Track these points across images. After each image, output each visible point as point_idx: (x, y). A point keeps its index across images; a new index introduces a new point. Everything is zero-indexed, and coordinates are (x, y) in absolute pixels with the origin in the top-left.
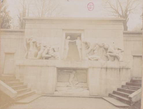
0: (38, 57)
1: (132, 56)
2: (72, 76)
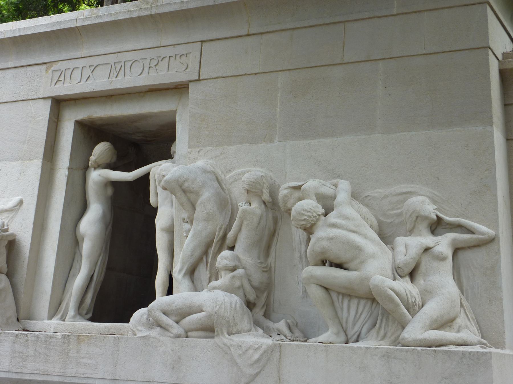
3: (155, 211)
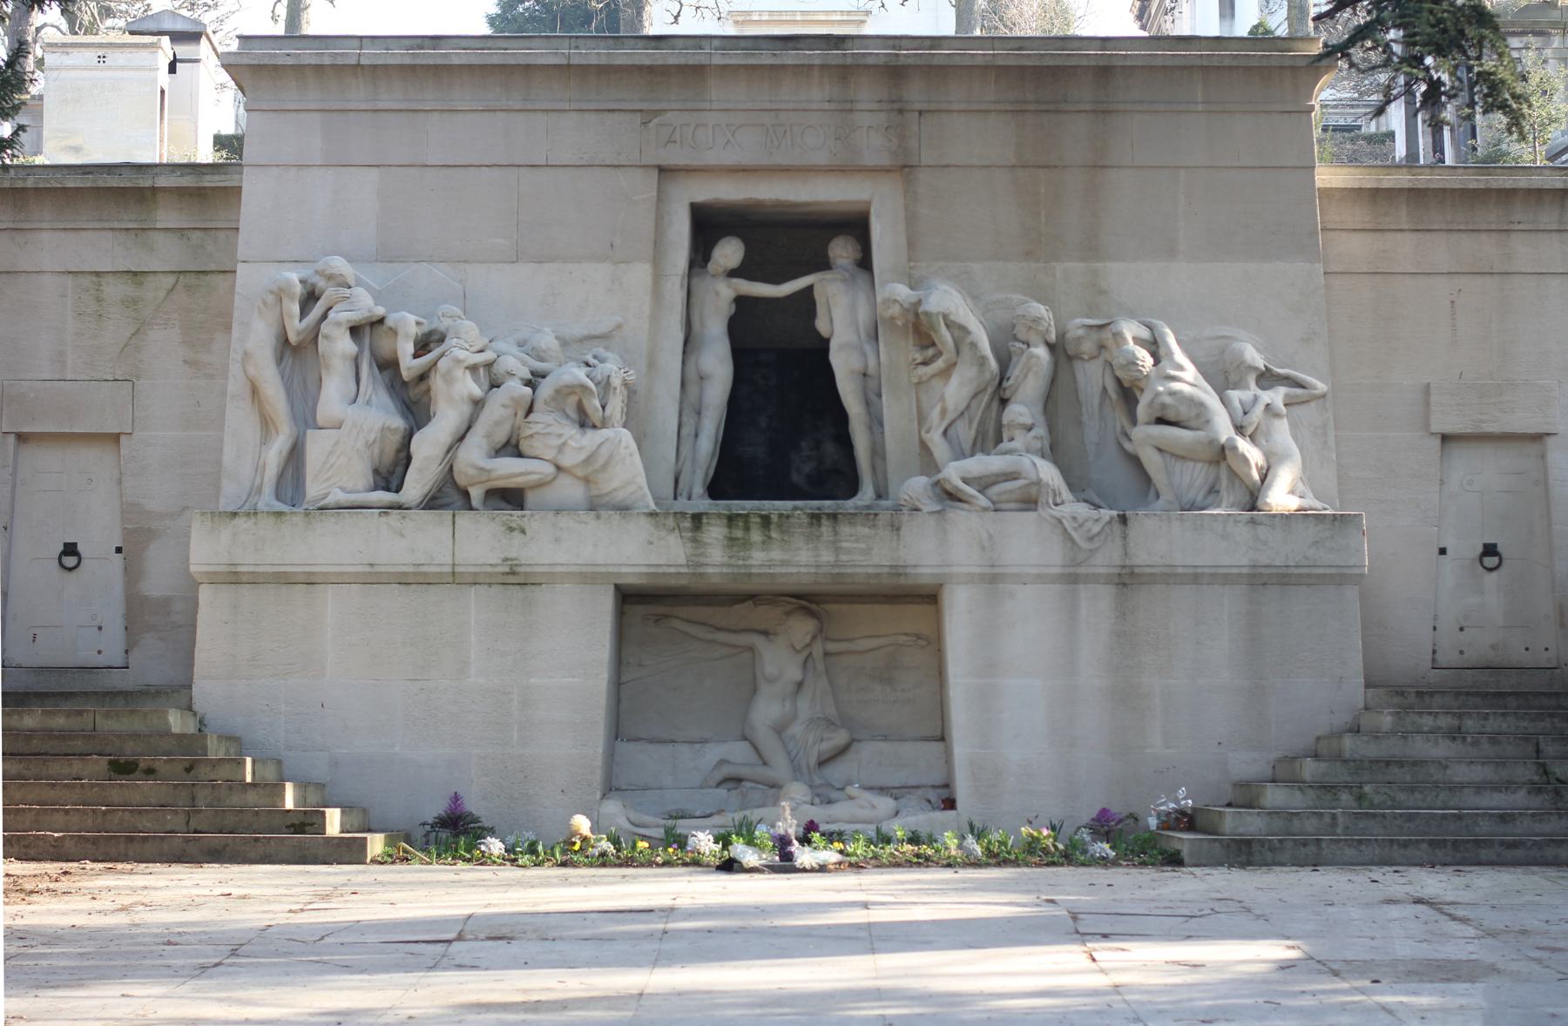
0: (416, 485)
1: (1436, 443)
2: (779, 660)
3: (822, 346)
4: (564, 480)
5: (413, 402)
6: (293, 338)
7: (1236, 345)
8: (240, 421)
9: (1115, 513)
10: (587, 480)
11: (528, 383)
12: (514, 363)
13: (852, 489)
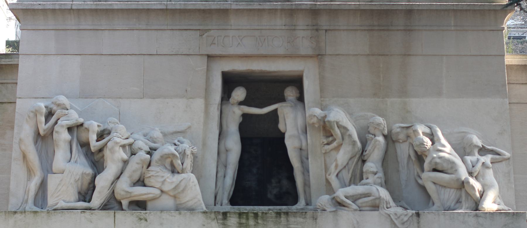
0: (97, 199)
3: (282, 136)
4: (165, 197)
5: (96, 162)
6: (42, 133)
7: (469, 136)
8: (18, 170)
9: (414, 212)
10: (175, 197)
11: (148, 153)
12: (142, 144)
13: (295, 200)
